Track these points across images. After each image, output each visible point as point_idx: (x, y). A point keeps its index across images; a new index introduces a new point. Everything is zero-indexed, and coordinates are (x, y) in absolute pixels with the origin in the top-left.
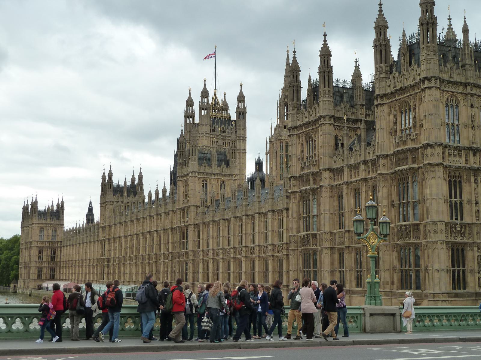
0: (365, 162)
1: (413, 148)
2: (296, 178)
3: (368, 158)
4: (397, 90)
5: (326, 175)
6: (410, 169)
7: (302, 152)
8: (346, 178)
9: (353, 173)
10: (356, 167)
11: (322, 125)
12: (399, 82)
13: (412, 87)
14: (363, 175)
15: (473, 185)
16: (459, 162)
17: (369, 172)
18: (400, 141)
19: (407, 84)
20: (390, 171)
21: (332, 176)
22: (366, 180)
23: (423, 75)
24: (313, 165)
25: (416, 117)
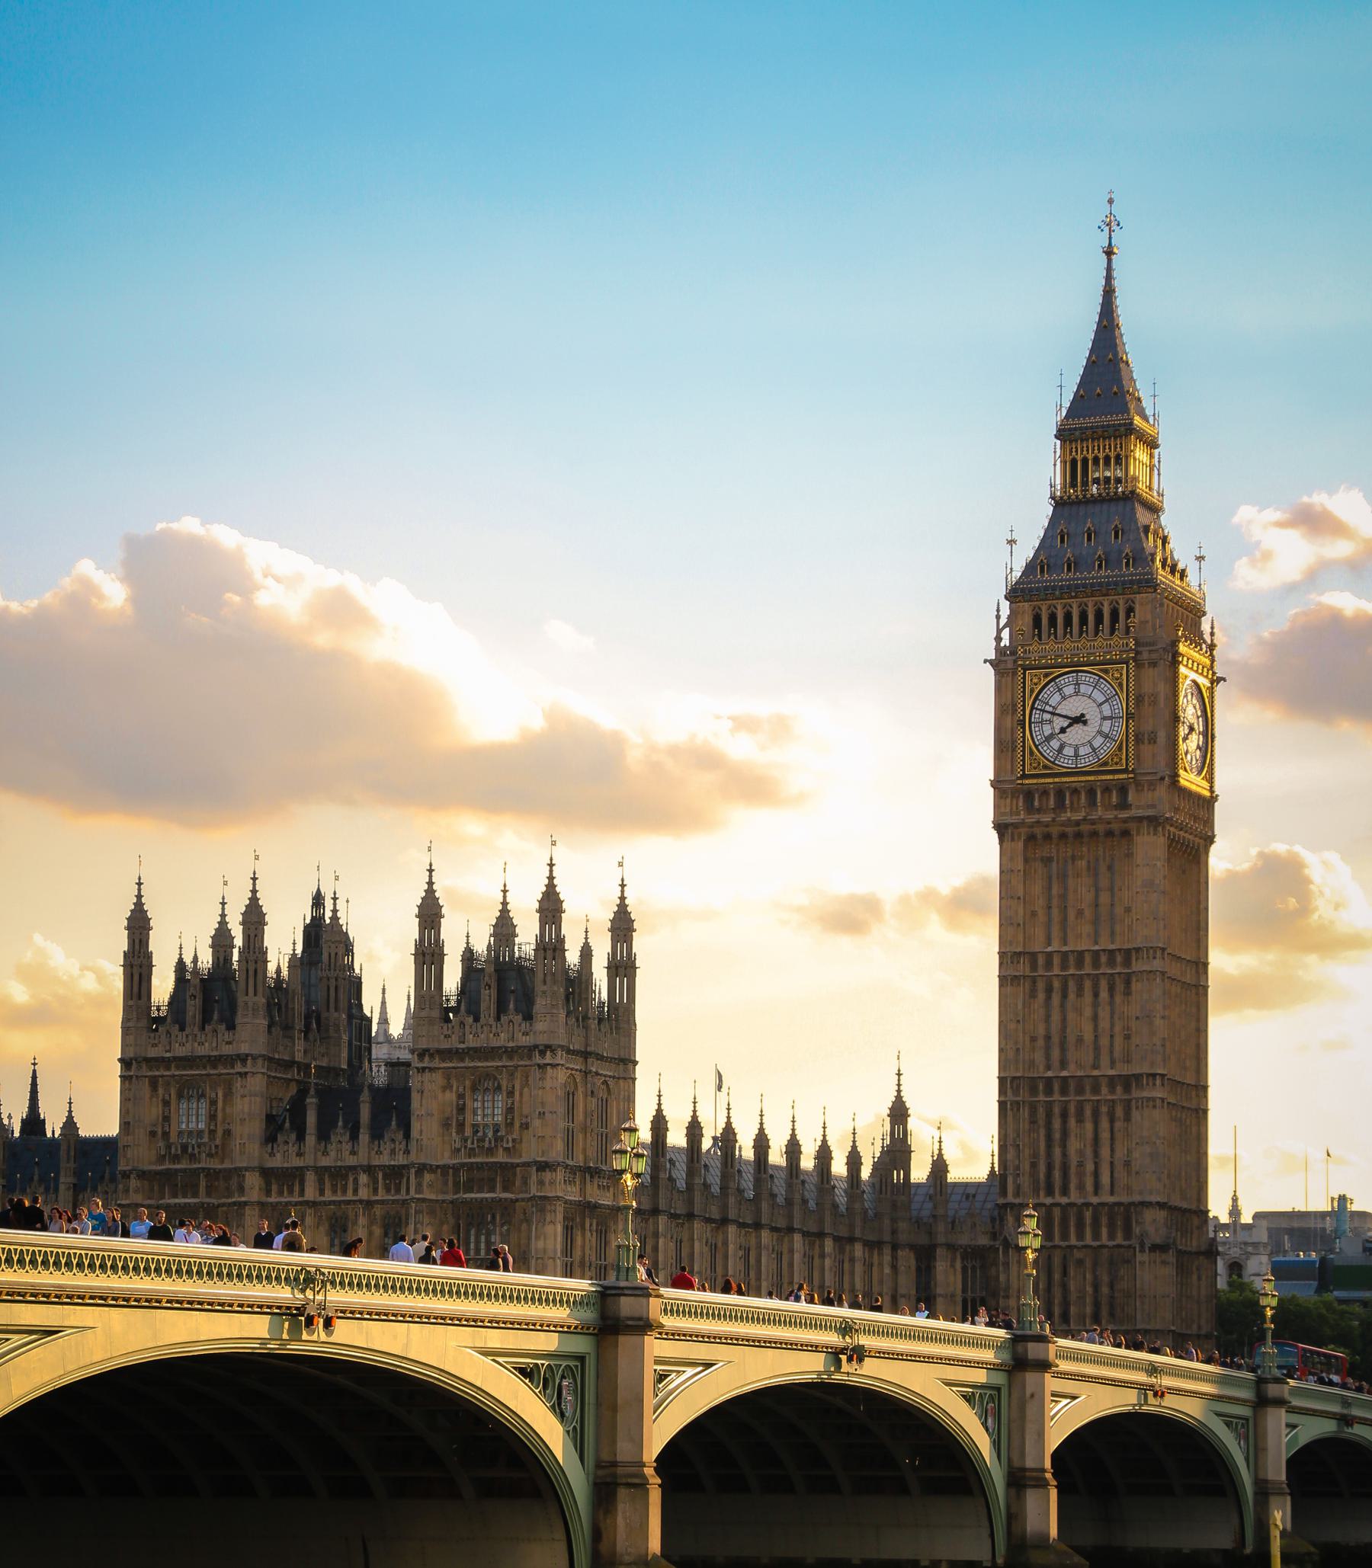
0: (369, 1169)
1: (506, 1163)
2: (142, 1175)
3: (377, 1163)
4: (469, 1049)
5: (253, 1181)
6: (501, 1199)
7: (166, 1119)
8: (310, 1193)
9: (328, 1185)
10: (339, 1175)
11: (249, 1075)
12: (476, 1035)
13: (510, 1053)
14: (364, 1194)
15: (588, 1234)
16: (573, 1194)
17: (375, 1191)
18: (478, 1146)
19: (495, 1043)
20: (450, 1197)
21: (264, 1186)
22: (369, 1204)
23: (542, 1040)
24: (210, 1155)
25: (513, 1108)
